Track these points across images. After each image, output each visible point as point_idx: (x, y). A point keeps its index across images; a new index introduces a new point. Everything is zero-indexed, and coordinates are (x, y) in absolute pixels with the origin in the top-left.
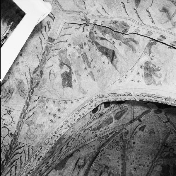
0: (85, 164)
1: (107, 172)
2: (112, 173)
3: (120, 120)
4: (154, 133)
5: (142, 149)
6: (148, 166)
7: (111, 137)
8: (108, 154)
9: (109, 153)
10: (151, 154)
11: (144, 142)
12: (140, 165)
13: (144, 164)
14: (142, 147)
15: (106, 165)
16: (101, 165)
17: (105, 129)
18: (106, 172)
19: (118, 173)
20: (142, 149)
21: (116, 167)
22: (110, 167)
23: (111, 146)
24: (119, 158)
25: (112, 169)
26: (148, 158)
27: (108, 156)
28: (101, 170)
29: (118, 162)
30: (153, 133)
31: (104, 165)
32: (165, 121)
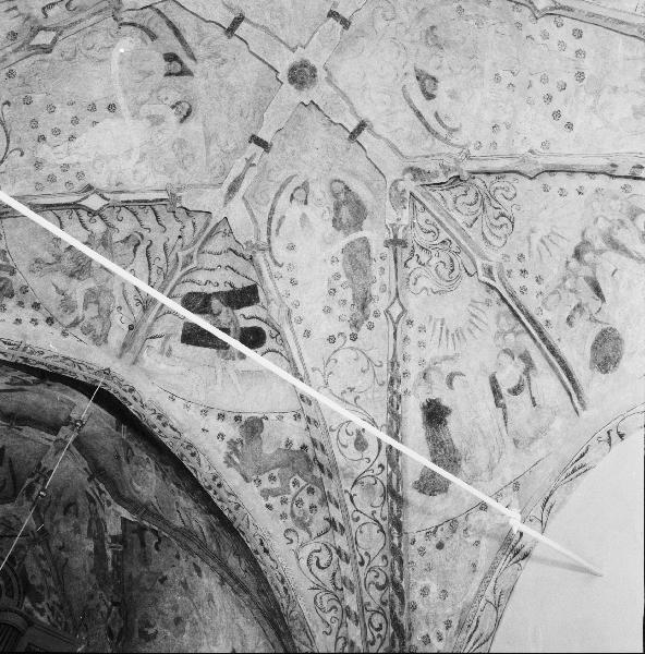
0: (525, 357)
1: (601, 252)
2: (610, 229)
3: (369, 208)
4: (433, 28)
5: (507, 78)
6: (578, 34)
7: (447, 230)
8: (529, 238)
9: (525, 233)
10: (519, 25)
11: (478, 71)
12: (580, 76)
13: (570, 53)
14: (497, 78)
15: (572, 253)
16: (565, 280)
17: (382, 269)
18: (599, 259)
20: (507, 78)
21: (588, 204)
22: (583, 234)
23: (498, 223)
24: (546, 189)
26: (539, 39)
27: (535, 240)
28: (585, 283)
30: (435, 32)
31: (567, 262)
32: (341, 27)
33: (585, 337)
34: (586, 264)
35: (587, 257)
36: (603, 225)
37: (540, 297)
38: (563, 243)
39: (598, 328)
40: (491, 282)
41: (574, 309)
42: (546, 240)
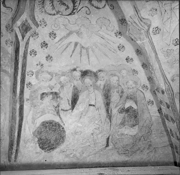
1: (96, 88)
8: (70, 33)
9: (75, 28)
16: (63, 74)
19: (135, 83)
22: (100, 71)
25: (113, 75)
27: (74, 38)
28: (71, 89)
29: (121, 48)
31: (75, 70)
33: (43, 113)
34: (83, 82)
35: (88, 80)
36: (114, 80)
37: (39, 67)
38: (84, 57)
39: (57, 119)
40: (20, 38)
41: (52, 93)
42: (78, 47)
